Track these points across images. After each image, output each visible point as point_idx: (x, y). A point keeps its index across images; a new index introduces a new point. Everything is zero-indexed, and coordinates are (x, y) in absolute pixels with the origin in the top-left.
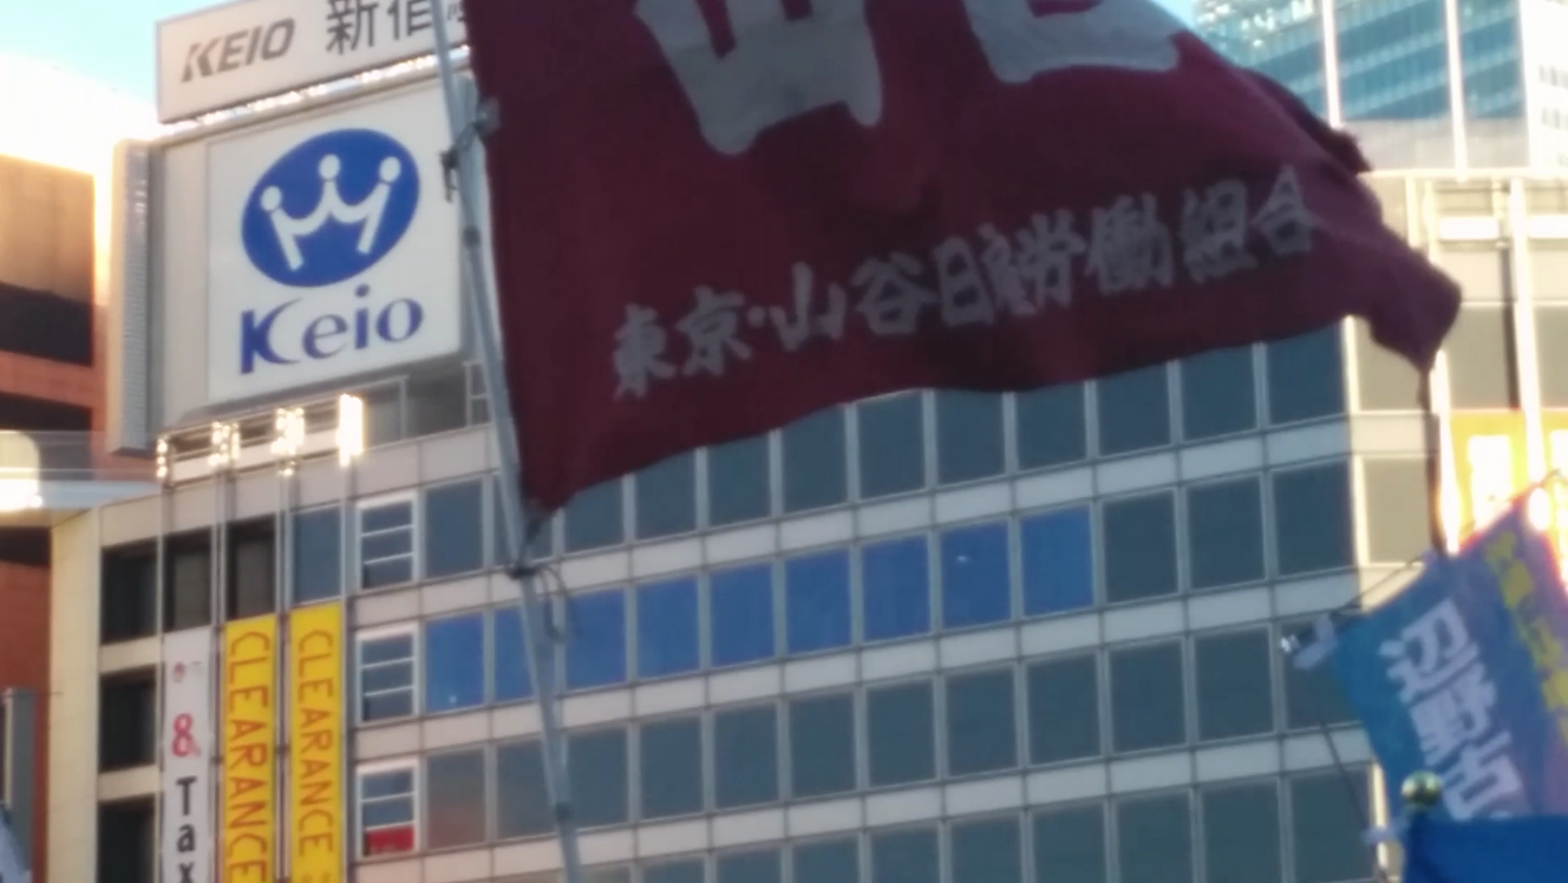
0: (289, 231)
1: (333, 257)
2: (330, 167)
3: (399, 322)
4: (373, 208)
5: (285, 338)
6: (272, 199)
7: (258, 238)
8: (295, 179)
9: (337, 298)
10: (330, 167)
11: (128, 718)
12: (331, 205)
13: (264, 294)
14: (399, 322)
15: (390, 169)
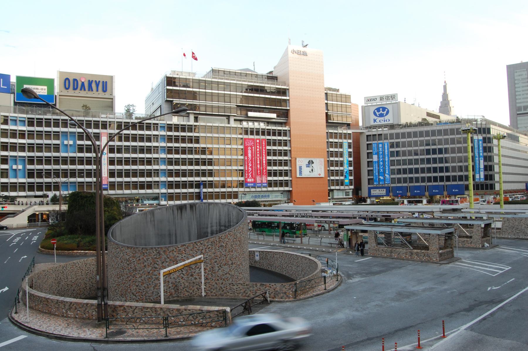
0: (377, 113)
1: (381, 115)
2: (381, 109)
3: (388, 120)
4: (385, 112)
5: (378, 121)
6: (376, 111)
7: (375, 114)
8: (378, 110)
9: (382, 118)
10: (381, 109)
11: (369, 146)
12: (381, 112)
13: (376, 118)
14: (388, 120)
15: (386, 110)
